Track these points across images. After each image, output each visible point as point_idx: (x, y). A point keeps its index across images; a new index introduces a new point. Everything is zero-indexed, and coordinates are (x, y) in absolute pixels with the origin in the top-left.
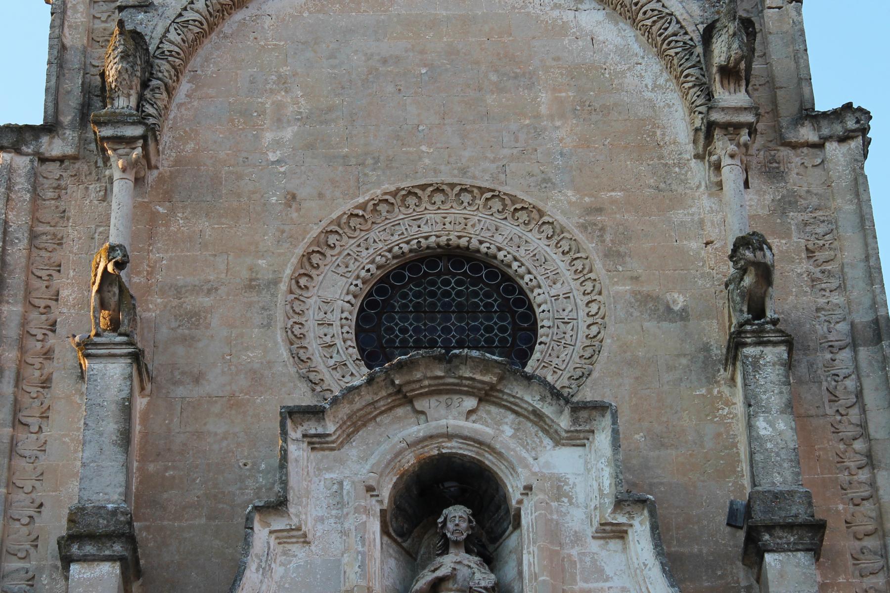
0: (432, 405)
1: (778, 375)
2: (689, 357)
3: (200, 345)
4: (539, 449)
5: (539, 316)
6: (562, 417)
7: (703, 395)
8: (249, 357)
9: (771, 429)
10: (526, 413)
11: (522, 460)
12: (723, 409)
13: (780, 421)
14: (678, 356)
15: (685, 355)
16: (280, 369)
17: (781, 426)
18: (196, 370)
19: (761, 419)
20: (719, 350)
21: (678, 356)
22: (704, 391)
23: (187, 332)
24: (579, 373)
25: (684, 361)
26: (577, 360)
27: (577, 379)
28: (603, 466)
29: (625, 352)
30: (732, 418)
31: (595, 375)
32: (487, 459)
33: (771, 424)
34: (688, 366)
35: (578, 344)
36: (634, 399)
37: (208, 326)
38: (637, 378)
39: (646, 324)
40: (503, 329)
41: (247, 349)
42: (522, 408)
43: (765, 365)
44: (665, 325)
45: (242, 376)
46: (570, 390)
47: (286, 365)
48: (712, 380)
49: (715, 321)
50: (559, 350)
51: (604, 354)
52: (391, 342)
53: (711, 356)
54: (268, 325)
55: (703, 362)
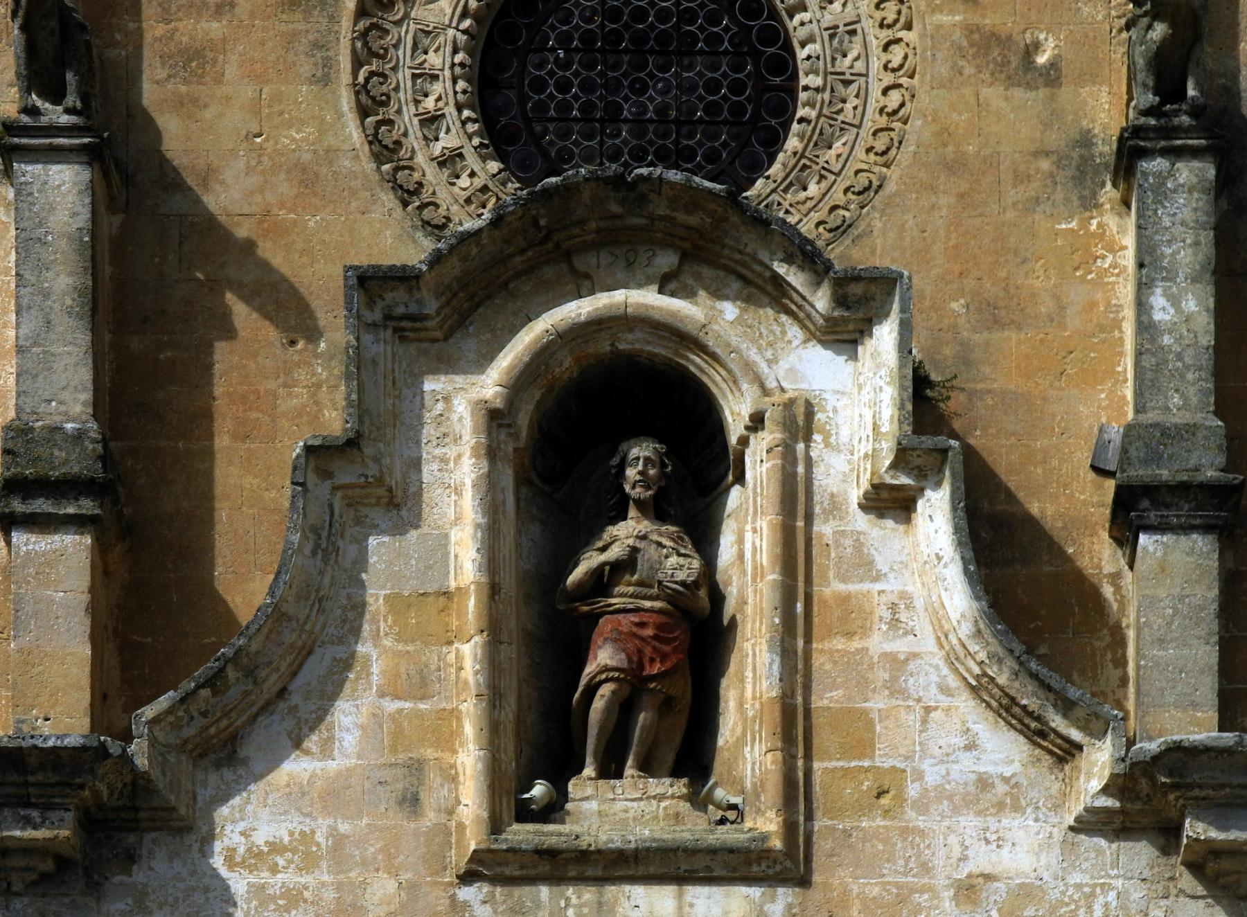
0: (603, 263)
1: (1195, 210)
2: (1055, 158)
3: (208, 114)
4: (780, 345)
5: (802, 66)
6: (820, 294)
7: (1072, 230)
8: (294, 140)
9: (1172, 311)
10: (760, 282)
11: (748, 366)
12: (1104, 257)
13: (1190, 296)
14: (1037, 154)
15: (1047, 154)
16: (347, 163)
17: (1191, 305)
18: (201, 163)
19: (1159, 291)
20: (1106, 148)
21: (1037, 154)
22: (1073, 225)
23: (183, 88)
24: (863, 180)
25: (1045, 165)
26: (862, 156)
27: (859, 193)
28: (882, 383)
29: (945, 145)
30: (1118, 275)
31: (890, 187)
32: (693, 363)
33: (1175, 301)
34: (1051, 175)
35: (868, 125)
36: (954, 235)
37: (219, 80)
38: (962, 196)
39: (986, 92)
40: (737, 88)
41: (289, 125)
42: (753, 271)
43: (1175, 191)
44: (1018, 93)
45: (282, 176)
46: (847, 214)
47: (358, 156)
48: (1089, 203)
49: (1105, 88)
50: (833, 134)
51: (909, 148)
52: (542, 107)
53: (1092, 157)
54: (325, 79)
55: (1078, 168)
